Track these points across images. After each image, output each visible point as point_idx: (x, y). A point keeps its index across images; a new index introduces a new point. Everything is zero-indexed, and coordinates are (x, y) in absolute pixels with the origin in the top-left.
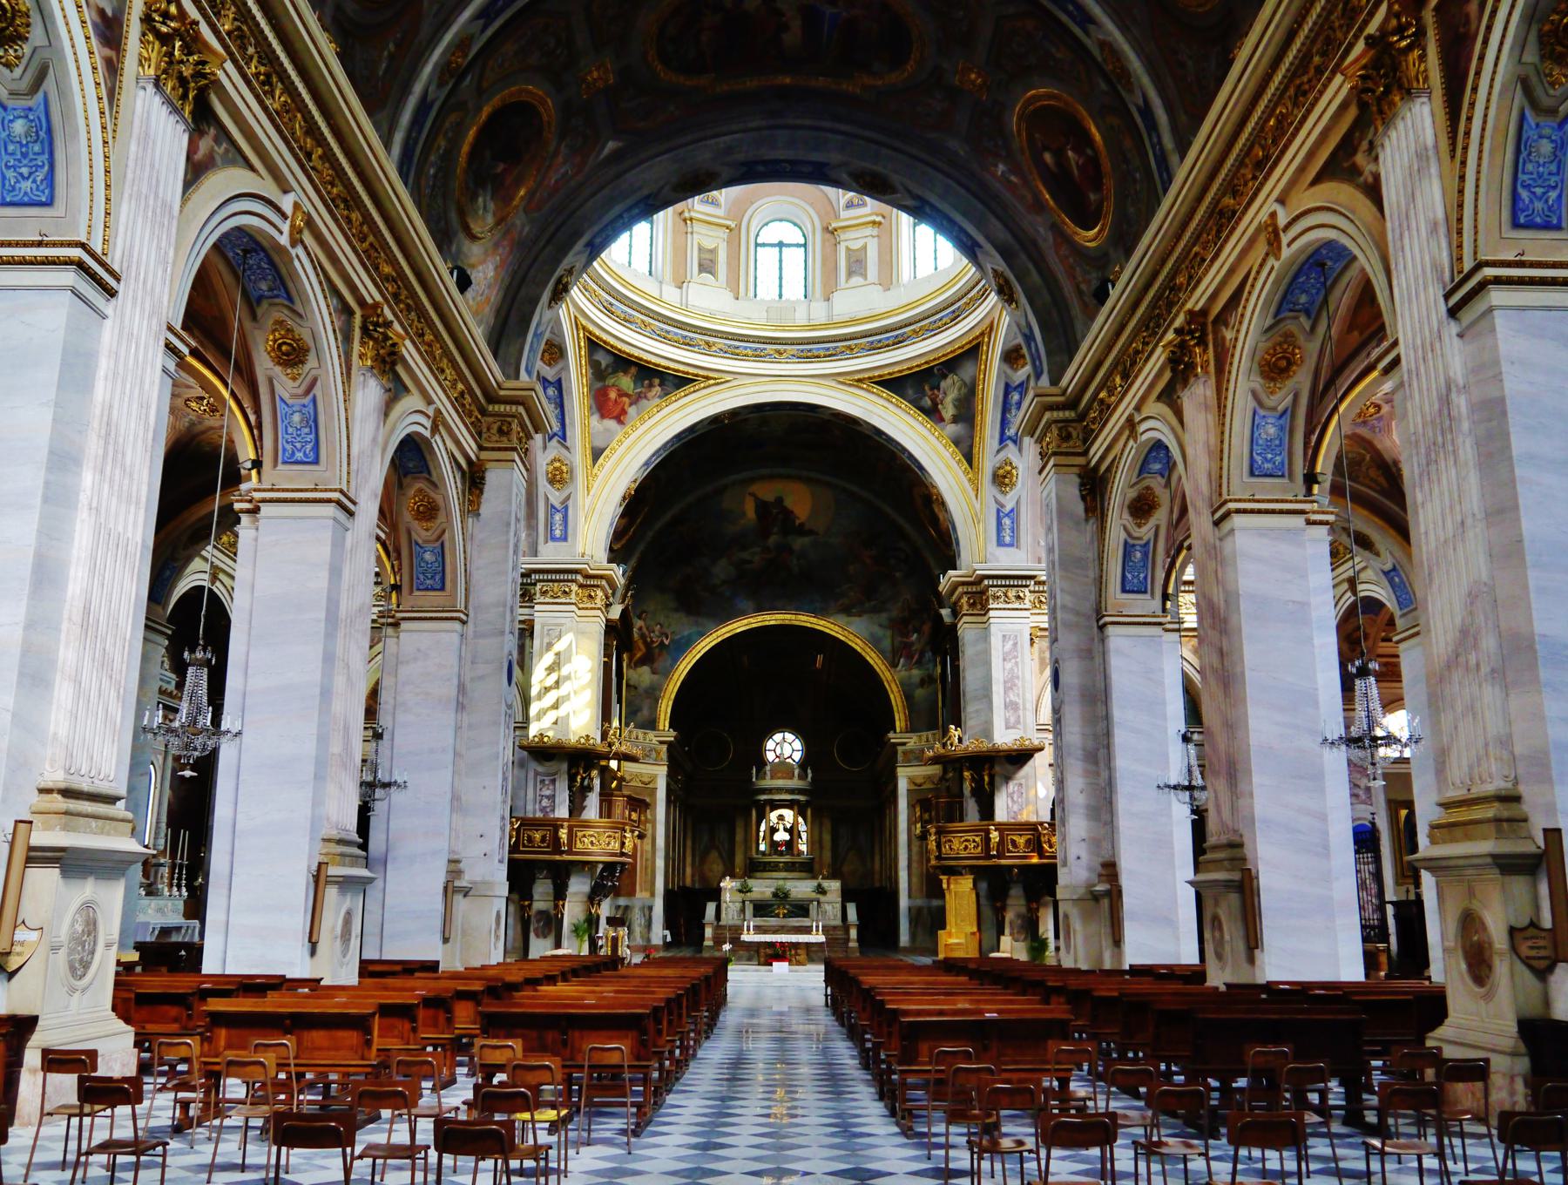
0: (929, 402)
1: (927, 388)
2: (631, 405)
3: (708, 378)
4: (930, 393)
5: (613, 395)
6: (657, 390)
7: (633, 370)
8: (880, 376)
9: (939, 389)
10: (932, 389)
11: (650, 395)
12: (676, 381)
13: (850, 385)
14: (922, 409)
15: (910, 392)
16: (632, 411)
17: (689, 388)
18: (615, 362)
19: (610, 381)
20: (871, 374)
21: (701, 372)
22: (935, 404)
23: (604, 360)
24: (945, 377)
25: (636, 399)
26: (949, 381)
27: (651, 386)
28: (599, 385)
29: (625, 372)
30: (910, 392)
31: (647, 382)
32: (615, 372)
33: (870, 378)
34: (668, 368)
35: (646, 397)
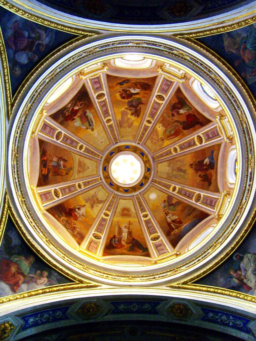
0: (236, 281)
1: (232, 273)
2: (24, 282)
3: (81, 282)
4: (235, 275)
5: (13, 269)
6: (45, 280)
7: (32, 259)
8: (197, 277)
9: (240, 270)
10: (235, 271)
11: (39, 281)
12: (59, 277)
13: (179, 288)
14: (234, 288)
15: (222, 280)
16: (24, 286)
17: (67, 285)
18: (21, 246)
19: (15, 259)
20: (192, 277)
21: (76, 276)
22: (241, 281)
23: (15, 241)
24: (242, 259)
25: (29, 281)
26: (245, 260)
27: (41, 276)
28: (7, 256)
29: (27, 258)
30: (222, 280)
31: (39, 272)
32: (19, 254)
33: (191, 280)
34: (56, 267)
35: (36, 282)
